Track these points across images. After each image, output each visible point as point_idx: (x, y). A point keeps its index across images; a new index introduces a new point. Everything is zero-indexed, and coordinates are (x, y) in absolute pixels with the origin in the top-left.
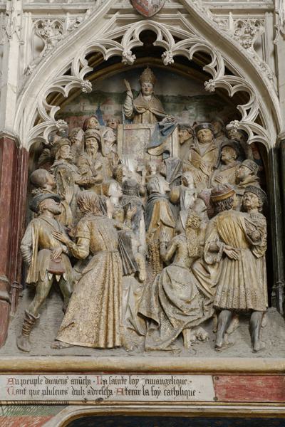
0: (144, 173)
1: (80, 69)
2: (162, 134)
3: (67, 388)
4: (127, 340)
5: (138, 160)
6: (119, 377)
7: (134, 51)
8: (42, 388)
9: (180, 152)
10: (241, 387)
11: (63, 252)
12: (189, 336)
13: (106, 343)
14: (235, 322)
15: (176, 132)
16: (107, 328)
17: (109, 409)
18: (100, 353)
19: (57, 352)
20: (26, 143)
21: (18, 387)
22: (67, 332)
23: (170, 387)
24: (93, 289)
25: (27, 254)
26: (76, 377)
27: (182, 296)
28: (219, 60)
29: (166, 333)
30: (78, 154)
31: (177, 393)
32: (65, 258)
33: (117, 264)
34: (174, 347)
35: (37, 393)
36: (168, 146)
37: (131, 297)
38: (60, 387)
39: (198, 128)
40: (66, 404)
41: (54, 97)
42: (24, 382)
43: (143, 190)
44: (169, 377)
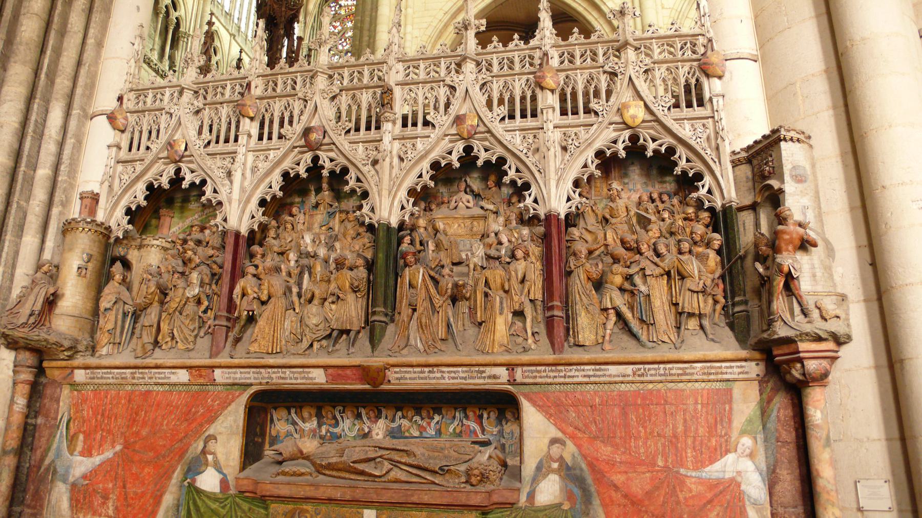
0: (317, 243)
3: (250, 376)
4: (284, 348)
6: (276, 370)
8: (239, 376)
9: (339, 227)
10: (339, 375)
11: (254, 298)
12: (316, 345)
13: (272, 351)
16: (273, 342)
17: (274, 387)
18: (269, 356)
19: (248, 356)
20: (244, 231)
21: (227, 375)
22: (253, 344)
23: (303, 375)
24: (268, 319)
27: (314, 322)
29: (305, 344)
31: (307, 379)
34: (307, 352)
35: (236, 378)
36: (331, 225)
37: (289, 323)
38: (247, 376)
40: (251, 385)
42: (229, 373)
44: (301, 370)
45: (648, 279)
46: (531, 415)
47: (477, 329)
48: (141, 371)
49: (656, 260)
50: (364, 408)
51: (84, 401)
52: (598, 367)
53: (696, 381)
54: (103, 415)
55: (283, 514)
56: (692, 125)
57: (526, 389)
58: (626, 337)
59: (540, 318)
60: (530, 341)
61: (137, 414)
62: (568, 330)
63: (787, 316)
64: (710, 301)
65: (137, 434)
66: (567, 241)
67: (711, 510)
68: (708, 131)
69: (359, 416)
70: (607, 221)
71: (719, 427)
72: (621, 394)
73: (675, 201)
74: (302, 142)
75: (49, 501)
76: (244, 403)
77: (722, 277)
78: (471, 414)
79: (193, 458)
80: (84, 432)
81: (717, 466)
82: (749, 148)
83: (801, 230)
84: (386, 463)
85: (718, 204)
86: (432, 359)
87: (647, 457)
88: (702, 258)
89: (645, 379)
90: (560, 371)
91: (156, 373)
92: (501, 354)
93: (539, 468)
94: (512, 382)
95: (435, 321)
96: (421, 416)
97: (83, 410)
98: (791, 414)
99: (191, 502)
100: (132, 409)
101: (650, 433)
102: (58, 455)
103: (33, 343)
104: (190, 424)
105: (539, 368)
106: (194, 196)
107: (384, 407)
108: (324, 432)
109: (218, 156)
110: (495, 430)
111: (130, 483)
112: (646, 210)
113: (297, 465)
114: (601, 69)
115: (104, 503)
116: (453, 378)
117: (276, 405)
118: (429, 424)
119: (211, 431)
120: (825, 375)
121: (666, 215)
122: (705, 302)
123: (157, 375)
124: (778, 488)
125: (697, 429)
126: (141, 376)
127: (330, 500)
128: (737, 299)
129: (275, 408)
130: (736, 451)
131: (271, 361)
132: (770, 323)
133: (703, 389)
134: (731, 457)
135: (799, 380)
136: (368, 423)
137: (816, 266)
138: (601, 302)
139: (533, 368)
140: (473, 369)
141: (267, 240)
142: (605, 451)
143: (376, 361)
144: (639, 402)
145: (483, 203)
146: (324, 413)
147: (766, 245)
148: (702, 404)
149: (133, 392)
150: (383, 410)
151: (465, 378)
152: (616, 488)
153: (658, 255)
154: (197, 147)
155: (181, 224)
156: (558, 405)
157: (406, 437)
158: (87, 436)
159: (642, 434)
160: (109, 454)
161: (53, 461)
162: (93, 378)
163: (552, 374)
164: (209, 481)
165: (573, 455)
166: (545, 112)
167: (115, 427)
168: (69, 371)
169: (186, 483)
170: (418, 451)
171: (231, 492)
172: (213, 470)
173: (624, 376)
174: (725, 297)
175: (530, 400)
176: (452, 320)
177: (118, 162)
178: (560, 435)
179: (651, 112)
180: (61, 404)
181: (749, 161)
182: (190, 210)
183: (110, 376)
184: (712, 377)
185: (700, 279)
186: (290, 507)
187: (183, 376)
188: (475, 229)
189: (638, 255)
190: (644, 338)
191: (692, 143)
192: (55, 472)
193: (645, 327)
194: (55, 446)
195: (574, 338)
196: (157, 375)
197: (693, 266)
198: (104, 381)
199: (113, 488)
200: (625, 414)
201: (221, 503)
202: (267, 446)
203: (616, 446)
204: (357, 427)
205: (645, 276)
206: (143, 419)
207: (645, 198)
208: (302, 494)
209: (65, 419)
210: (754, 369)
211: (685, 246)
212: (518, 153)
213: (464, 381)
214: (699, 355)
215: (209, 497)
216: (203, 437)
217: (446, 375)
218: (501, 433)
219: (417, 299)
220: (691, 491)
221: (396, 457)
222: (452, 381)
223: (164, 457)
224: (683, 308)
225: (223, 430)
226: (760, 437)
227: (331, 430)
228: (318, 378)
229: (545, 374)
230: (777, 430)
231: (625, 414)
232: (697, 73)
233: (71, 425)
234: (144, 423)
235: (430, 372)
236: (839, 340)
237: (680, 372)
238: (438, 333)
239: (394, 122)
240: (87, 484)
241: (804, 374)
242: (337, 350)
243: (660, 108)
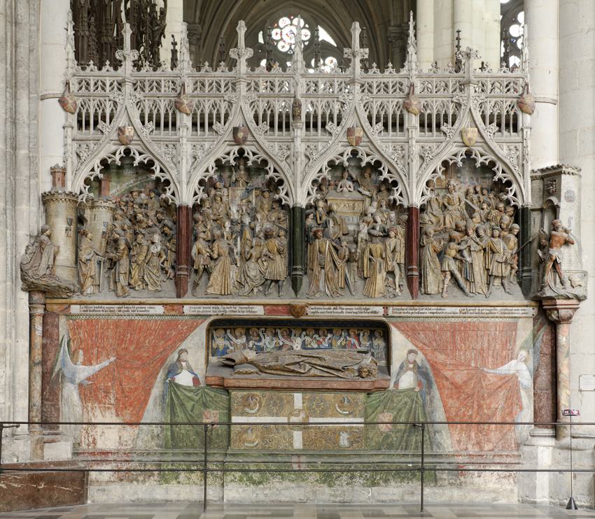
1: (213, 168)
2: (248, 192)
3: (210, 310)
4: (232, 291)
5: (238, 205)
7: (235, 159)
8: (201, 310)
10: (274, 310)
12: (255, 290)
14: (273, 284)
15: (254, 191)
17: (226, 317)
18: (222, 297)
25: (194, 257)
26: (214, 306)
28: (271, 165)
29: (247, 288)
30: (213, 202)
32: (209, 258)
33: (229, 260)
36: (250, 199)
37: (234, 273)
39: (264, 192)
40: (210, 316)
41: (201, 183)
43: (239, 222)
45: (472, 253)
46: (397, 337)
47: (363, 282)
48: (126, 306)
49: (478, 240)
51: (79, 327)
52: (439, 308)
53: (497, 317)
54: (96, 336)
56: (508, 147)
57: (394, 320)
58: (456, 289)
59: (403, 275)
60: (398, 290)
61: (124, 336)
62: (420, 283)
63: (552, 284)
64: (509, 268)
65: (126, 349)
66: (421, 223)
67: (500, 392)
68: (518, 153)
69: (276, 335)
70: (445, 207)
71: (508, 344)
72: (453, 325)
73: (492, 196)
74: (231, 137)
75: (62, 395)
76: (205, 328)
77: (518, 253)
78: (352, 333)
80: (83, 349)
81: (506, 367)
82: (542, 170)
83: (565, 235)
84: (307, 365)
85: (520, 204)
86: (337, 302)
87: (466, 361)
88: (506, 240)
89: (467, 315)
92: (380, 298)
93: (401, 367)
94: (386, 315)
95: (336, 276)
96: (319, 334)
97: (79, 333)
98: (550, 338)
100: (120, 332)
101: (469, 347)
102: (64, 364)
103: (50, 288)
104: (167, 342)
105: (403, 308)
106: (128, 164)
108: (251, 345)
109: (162, 143)
110: (368, 344)
112: (472, 201)
113: (244, 367)
114: (450, 99)
115: (106, 396)
116: (349, 313)
117: (217, 327)
118: (324, 340)
119: (183, 346)
120: (570, 318)
121: (485, 206)
122: (506, 268)
123: (139, 309)
124: (539, 379)
125: (495, 345)
127: (273, 388)
128: (525, 268)
129: (216, 330)
130: (517, 358)
131: (227, 301)
132: (542, 288)
133: (500, 322)
134: (513, 362)
135: (555, 320)
136: (282, 339)
137: (572, 255)
138: (441, 266)
139: (400, 308)
140: (362, 307)
141: (203, 209)
142: (441, 357)
143: (299, 302)
144: (462, 328)
145: (361, 189)
146: (251, 333)
147: (545, 239)
148: (499, 331)
149: (119, 320)
150: (293, 330)
151: (356, 313)
152: (447, 379)
153: (478, 236)
154: (145, 133)
155: (118, 188)
156: (414, 330)
157: (310, 349)
158: (86, 351)
159: (463, 348)
160: (106, 363)
161: (61, 369)
162: (87, 311)
163: (411, 311)
164: (184, 379)
165: (422, 360)
166: (410, 131)
167: (108, 345)
169: (167, 381)
170: (327, 358)
173: (454, 313)
174: (518, 265)
175: (396, 326)
176: (348, 276)
177: (73, 140)
178: (414, 348)
179: (482, 137)
180: (60, 329)
181: (542, 178)
182: (125, 176)
183: (101, 309)
184: (506, 315)
185: (504, 255)
186: (245, 393)
187: (160, 310)
188: (356, 209)
189: (466, 236)
190: (467, 290)
191: (507, 161)
192: (63, 376)
193: (468, 283)
194: (60, 359)
195: (425, 289)
196: (139, 309)
197: (500, 245)
198: (95, 313)
200: (453, 336)
202: (210, 355)
203: (447, 355)
204: (274, 342)
205: (470, 251)
206: (130, 339)
207: (472, 190)
208: (255, 385)
209: (66, 340)
210: (532, 311)
211: (496, 233)
212: (392, 161)
213: (355, 315)
214: (499, 303)
215: (185, 389)
216: (177, 350)
217: (344, 311)
218: (371, 345)
219: (324, 262)
220: (489, 381)
221: (314, 361)
222: (348, 314)
223: (149, 364)
224: (492, 272)
226: (531, 351)
228: (259, 312)
230: (541, 347)
231: (453, 336)
232: (515, 107)
233: (71, 343)
234: (131, 342)
235: (334, 308)
236: (579, 299)
237: (488, 312)
238: (338, 283)
239: (301, 129)
240: (91, 384)
241: (558, 317)
242: (271, 293)
243: (488, 133)
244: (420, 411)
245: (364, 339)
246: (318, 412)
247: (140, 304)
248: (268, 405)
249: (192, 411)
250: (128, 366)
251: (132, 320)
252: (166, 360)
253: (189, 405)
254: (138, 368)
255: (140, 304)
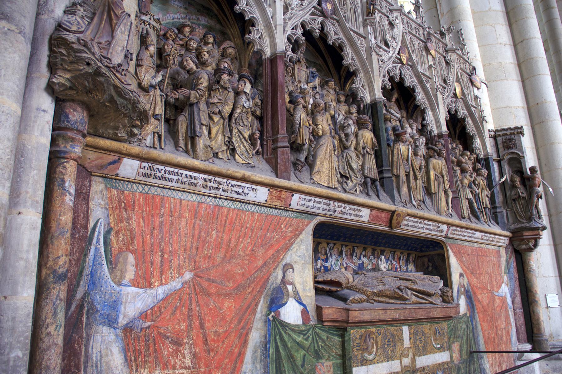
17: (335, 221)
21: (302, 202)
38: (319, 205)
40: (317, 215)
42: (305, 200)
50: (346, 246)
55: (359, 338)
79: (274, 289)
90: (463, 232)
91: (234, 185)
93: (458, 291)
99: (278, 338)
103: (119, 100)
107: (357, 247)
111: (209, 321)
115: (177, 351)
123: (235, 189)
126: (215, 185)
136: (346, 260)
146: (319, 249)
151: (431, 230)
162: (149, 176)
163: (460, 233)
168: (112, 157)
169: (270, 317)
171: (311, 323)
172: (294, 301)
183: (175, 178)
196: (235, 189)
199: (188, 330)
201: (304, 335)
204: (339, 263)
215: (293, 330)
216: (281, 266)
223: (244, 288)
225: (298, 258)
227: (324, 264)
229: (457, 233)
244: (472, 337)
245: (403, 263)
246: (421, 348)
247: (244, 179)
248: (383, 346)
249: (303, 366)
250: (213, 290)
251: (220, 207)
252: (268, 278)
253: (299, 356)
254: (228, 295)
255: (244, 179)
